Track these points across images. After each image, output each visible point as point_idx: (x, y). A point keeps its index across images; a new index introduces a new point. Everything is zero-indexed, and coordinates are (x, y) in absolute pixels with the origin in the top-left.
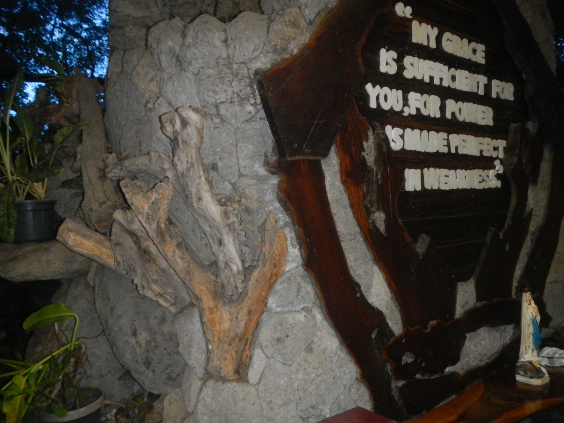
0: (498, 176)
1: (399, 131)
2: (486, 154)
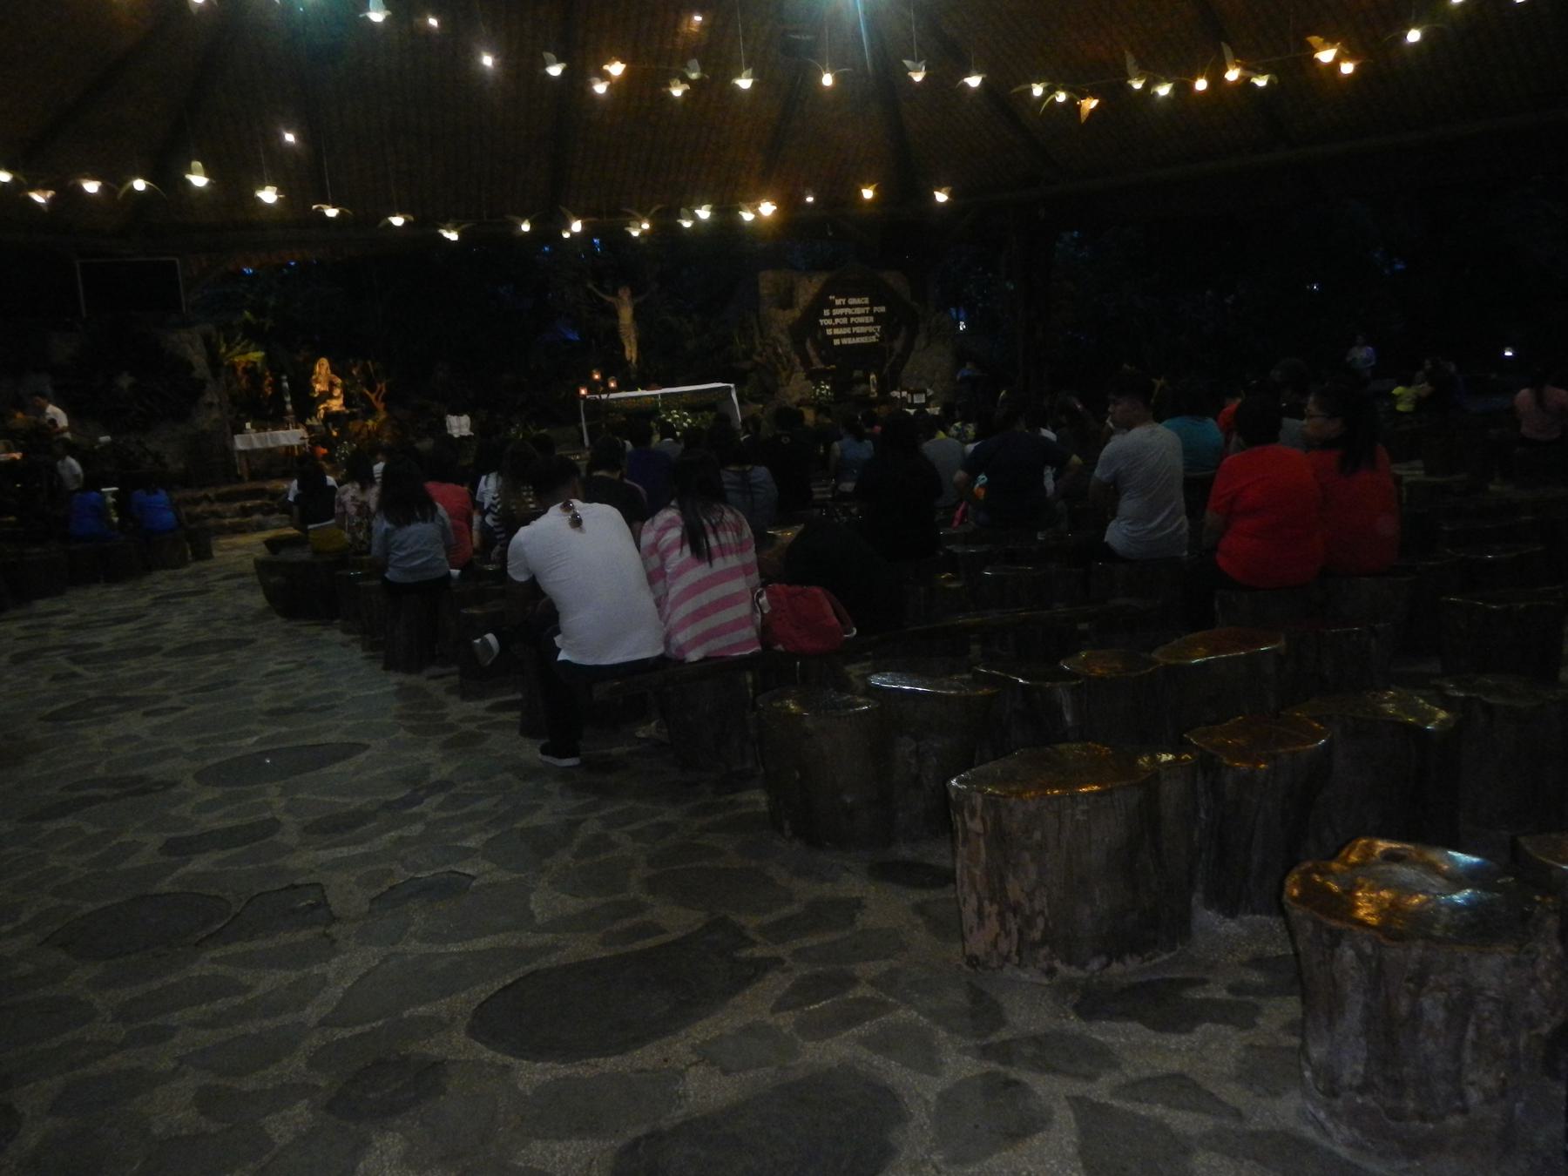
0: (877, 338)
1: (831, 330)
2: (870, 331)
